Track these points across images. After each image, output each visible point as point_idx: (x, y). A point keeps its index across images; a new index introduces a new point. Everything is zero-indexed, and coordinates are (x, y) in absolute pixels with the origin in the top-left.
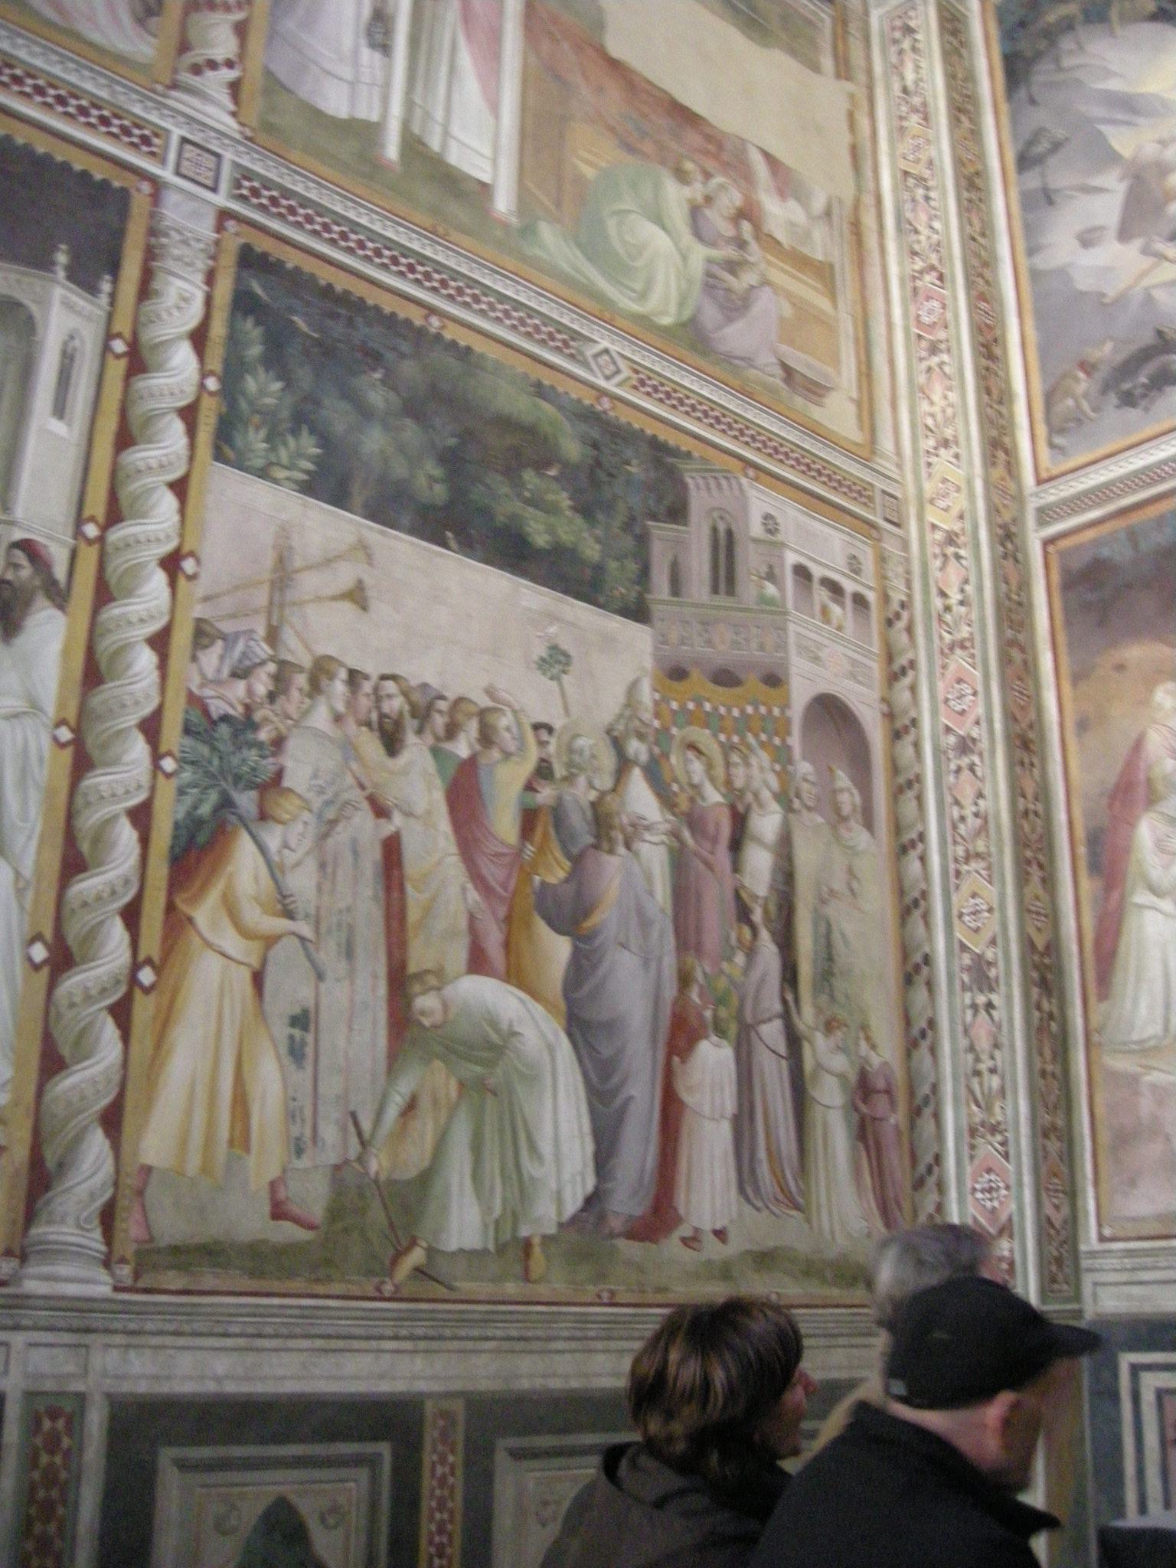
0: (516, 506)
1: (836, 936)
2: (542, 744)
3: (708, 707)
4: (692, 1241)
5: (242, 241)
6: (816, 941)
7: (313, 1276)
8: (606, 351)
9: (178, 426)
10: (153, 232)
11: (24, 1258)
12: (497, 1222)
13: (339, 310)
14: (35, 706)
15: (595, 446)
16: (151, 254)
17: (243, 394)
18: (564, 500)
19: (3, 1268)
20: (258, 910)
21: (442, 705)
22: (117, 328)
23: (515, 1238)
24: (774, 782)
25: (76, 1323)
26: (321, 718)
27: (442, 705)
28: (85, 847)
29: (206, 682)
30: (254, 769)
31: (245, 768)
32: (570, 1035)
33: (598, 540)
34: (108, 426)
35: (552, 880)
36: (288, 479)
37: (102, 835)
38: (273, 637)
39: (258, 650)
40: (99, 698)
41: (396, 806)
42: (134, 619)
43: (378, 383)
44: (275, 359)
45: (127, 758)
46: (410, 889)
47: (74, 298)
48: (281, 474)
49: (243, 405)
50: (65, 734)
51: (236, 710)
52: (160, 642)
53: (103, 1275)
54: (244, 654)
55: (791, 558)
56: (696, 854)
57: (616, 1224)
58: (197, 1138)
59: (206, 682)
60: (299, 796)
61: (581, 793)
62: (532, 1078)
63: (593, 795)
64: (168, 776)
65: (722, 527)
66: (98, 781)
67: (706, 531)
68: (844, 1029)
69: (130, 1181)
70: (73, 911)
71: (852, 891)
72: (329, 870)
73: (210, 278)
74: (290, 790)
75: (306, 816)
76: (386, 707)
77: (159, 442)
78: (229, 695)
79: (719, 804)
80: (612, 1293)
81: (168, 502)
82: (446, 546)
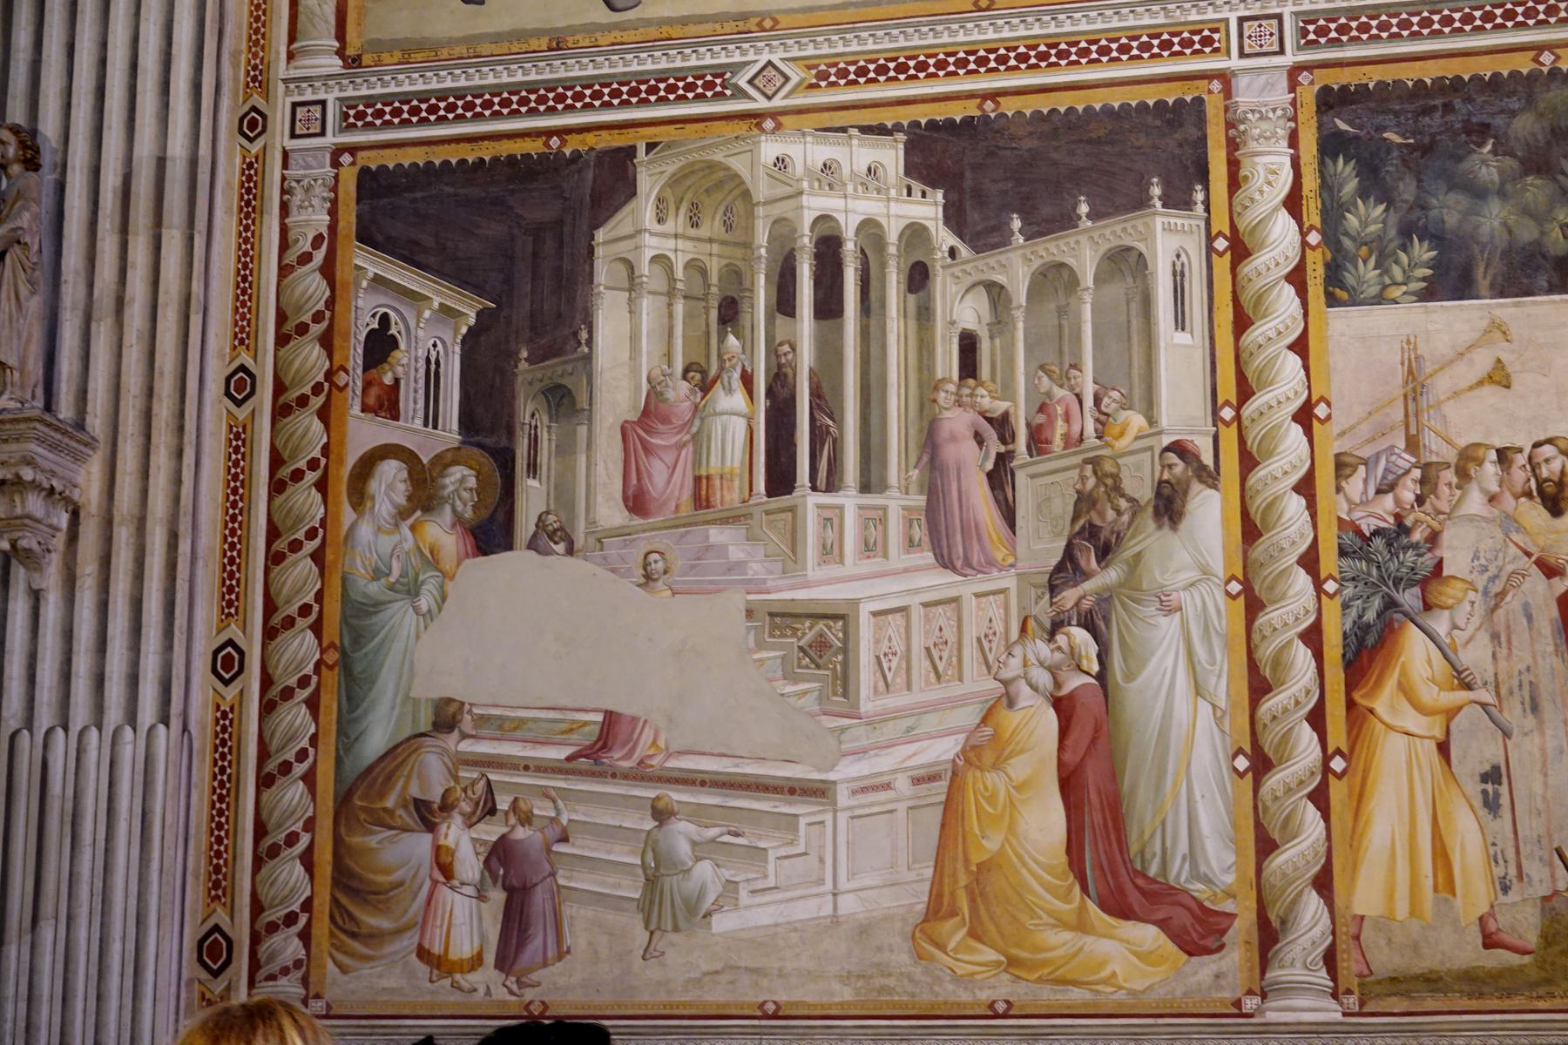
5: (1316, 88)
7: (1535, 995)
9: (1289, 290)
10: (1230, 125)
11: (1264, 996)
13: (1433, 103)
14: (1206, 572)
16: (1233, 145)
17: (1347, 234)
19: (1250, 1004)
20: (1436, 689)
22: (1214, 232)
26: (1475, 502)
28: (1267, 673)
29: (1353, 506)
30: (1413, 569)
31: (1404, 570)
34: (1225, 316)
36: (1405, 293)
37: (1278, 661)
38: (1413, 445)
39: (1401, 462)
40: (1259, 550)
42: (1279, 475)
43: (1490, 156)
44: (1374, 184)
45: (1291, 592)
47: (1172, 221)
48: (1396, 292)
49: (1347, 243)
50: (1235, 587)
52: (1306, 486)
53: (1333, 1004)
54: (1386, 470)
59: (1353, 506)
64: (1331, 596)
66: (1270, 617)
70: (1265, 725)
72: (1503, 639)
73: (1293, 140)
74: (1453, 577)
75: (1472, 595)
76: (1545, 473)
81: (1294, 361)
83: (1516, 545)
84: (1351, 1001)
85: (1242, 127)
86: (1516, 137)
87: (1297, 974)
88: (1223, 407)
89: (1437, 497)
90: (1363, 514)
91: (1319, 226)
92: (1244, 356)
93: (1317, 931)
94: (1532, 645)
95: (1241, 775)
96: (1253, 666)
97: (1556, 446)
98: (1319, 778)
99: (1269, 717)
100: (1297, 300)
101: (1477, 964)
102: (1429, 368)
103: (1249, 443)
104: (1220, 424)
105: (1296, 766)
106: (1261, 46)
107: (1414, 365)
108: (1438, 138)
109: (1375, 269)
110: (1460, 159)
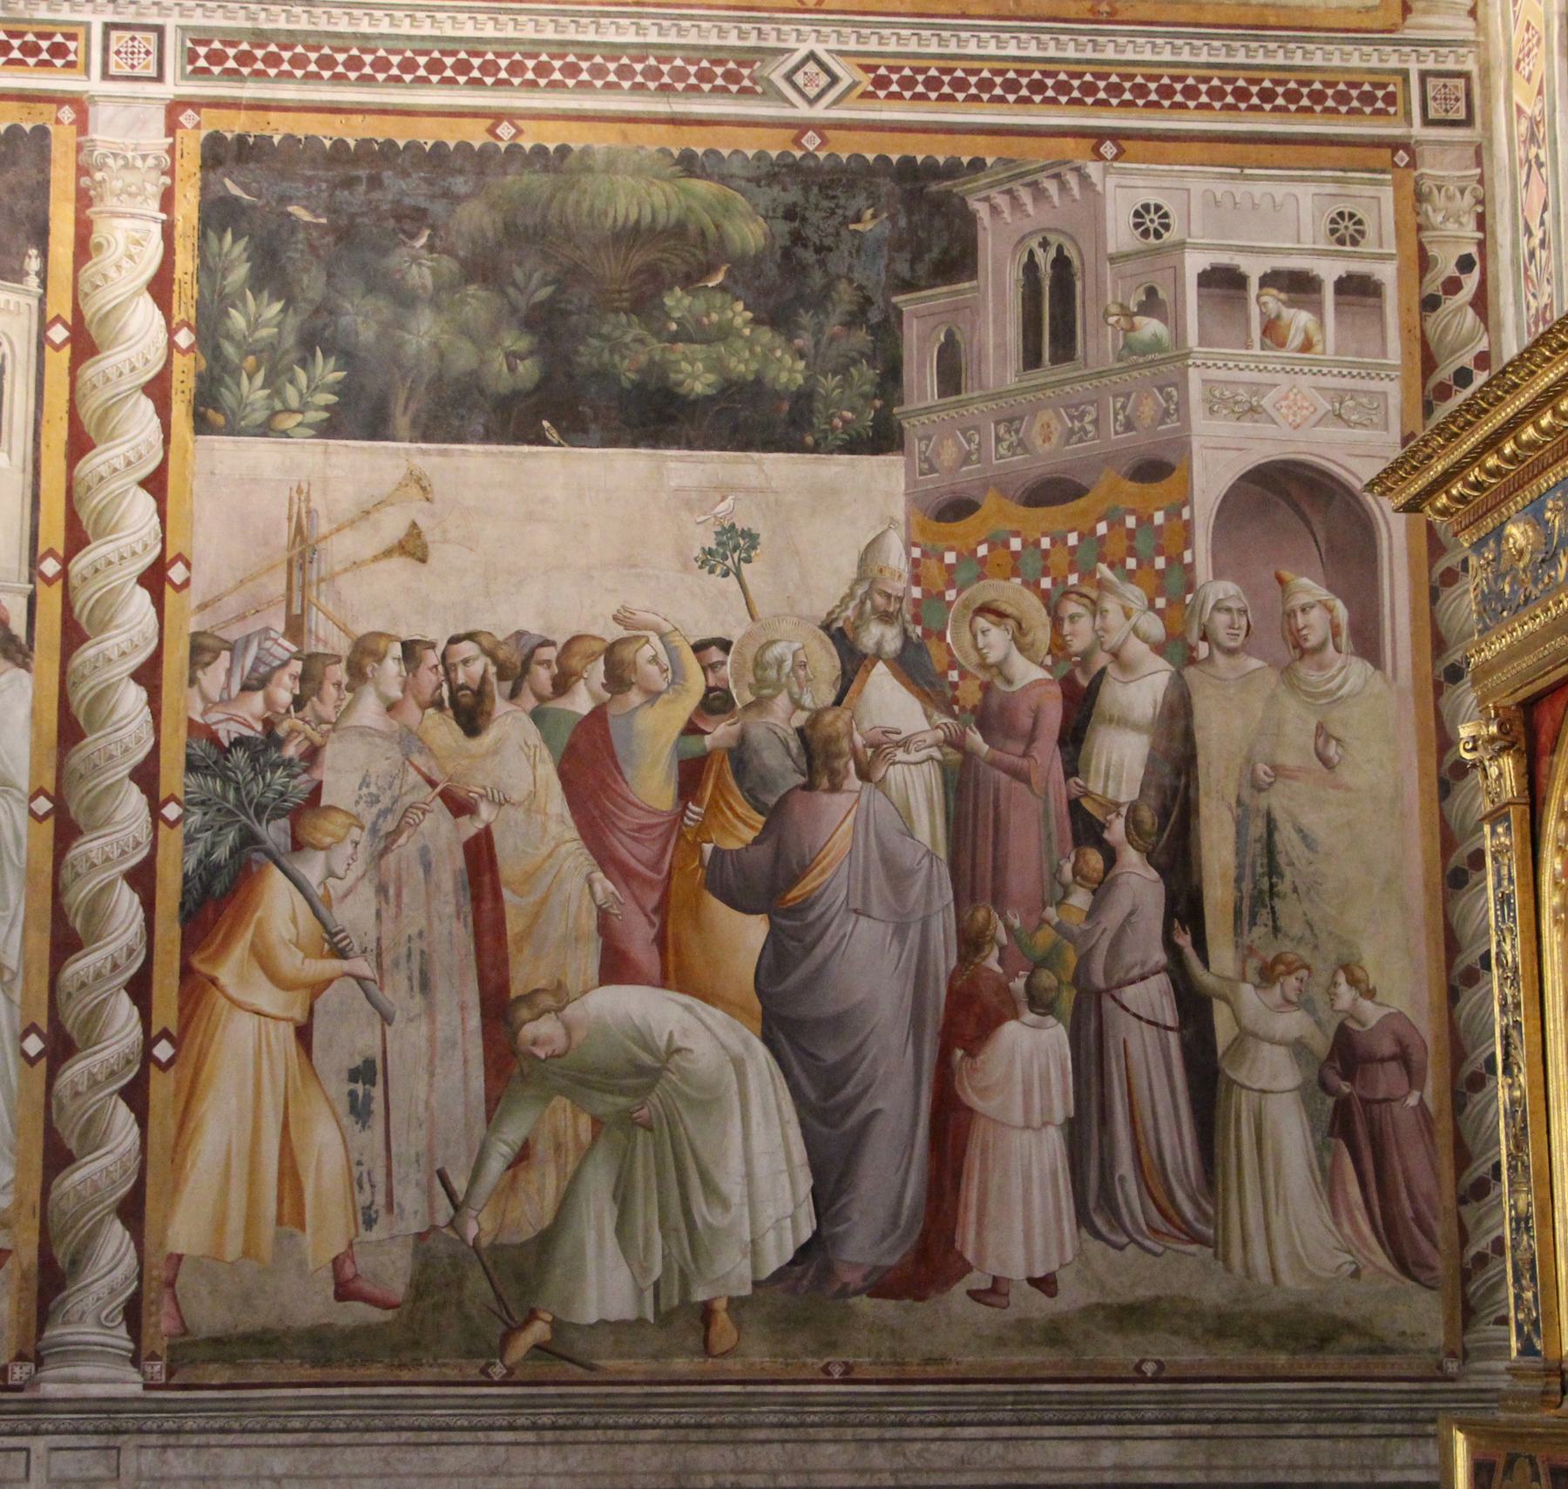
0: (656, 346)
1: (1286, 837)
2: (707, 668)
3: (1016, 544)
4: (995, 1292)
5: (204, 133)
6: (1239, 851)
8: (812, 56)
9: (147, 406)
10: (82, 170)
11: (39, 1362)
12: (657, 1285)
13: (355, 173)
15: (790, 214)
16: (84, 199)
17: (229, 337)
18: (739, 314)
19: (18, 1373)
20: (301, 955)
21: (549, 653)
22: (51, 314)
23: (685, 1301)
24: (1155, 627)
25: (105, 1425)
26: (369, 710)
27: (549, 653)
28: (78, 924)
30: (282, 794)
31: (270, 795)
32: (767, 1040)
33: (801, 355)
35: (732, 844)
36: (299, 424)
37: (96, 908)
38: (295, 628)
40: (76, 759)
41: (481, 796)
42: (114, 656)
43: (424, 252)
45: (118, 817)
46: (506, 893)
48: (289, 422)
49: (229, 349)
50: (43, 805)
51: (252, 728)
52: (149, 675)
53: (132, 1373)
54: (258, 659)
55: (1195, 263)
56: (994, 764)
57: (853, 1278)
58: (235, 1222)
60: (346, 813)
61: (782, 717)
62: (707, 1102)
63: (800, 718)
64: (172, 825)
65: (1044, 260)
66: (88, 847)
67: (1013, 274)
68: (1303, 973)
69: (159, 1272)
70: (69, 995)
71: (1326, 762)
72: (392, 891)
73: (167, 200)
74: (332, 808)
75: (355, 832)
76: (461, 678)
77: (127, 432)
78: (243, 713)
79: (1038, 683)
80: (848, 1368)
82: (544, 441)
83: (418, 769)
84: (157, 1368)
85: (98, 176)
86: (458, 231)
87: (87, 1332)
88: (44, 557)
89: (321, 700)
90: (221, 717)
91: (193, 322)
92: (79, 490)
93: (119, 1273)
94: (428, 903)
95: (32, 1061)
96: (59, 913)
97: (480, 644)
98: (136, 1069)
99: (76, 984)
100: (156, 421)
101: (325, 1321)
102: (324, 527)
103: (77, 610)
104: (38, 580)
105: (106, 1052)
106: (133, 67)
107: (304, 521)
108: (359, 220)
109: (263, 387)
110: (384, 252)
